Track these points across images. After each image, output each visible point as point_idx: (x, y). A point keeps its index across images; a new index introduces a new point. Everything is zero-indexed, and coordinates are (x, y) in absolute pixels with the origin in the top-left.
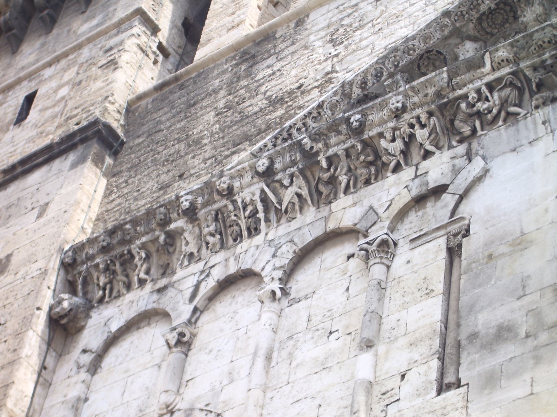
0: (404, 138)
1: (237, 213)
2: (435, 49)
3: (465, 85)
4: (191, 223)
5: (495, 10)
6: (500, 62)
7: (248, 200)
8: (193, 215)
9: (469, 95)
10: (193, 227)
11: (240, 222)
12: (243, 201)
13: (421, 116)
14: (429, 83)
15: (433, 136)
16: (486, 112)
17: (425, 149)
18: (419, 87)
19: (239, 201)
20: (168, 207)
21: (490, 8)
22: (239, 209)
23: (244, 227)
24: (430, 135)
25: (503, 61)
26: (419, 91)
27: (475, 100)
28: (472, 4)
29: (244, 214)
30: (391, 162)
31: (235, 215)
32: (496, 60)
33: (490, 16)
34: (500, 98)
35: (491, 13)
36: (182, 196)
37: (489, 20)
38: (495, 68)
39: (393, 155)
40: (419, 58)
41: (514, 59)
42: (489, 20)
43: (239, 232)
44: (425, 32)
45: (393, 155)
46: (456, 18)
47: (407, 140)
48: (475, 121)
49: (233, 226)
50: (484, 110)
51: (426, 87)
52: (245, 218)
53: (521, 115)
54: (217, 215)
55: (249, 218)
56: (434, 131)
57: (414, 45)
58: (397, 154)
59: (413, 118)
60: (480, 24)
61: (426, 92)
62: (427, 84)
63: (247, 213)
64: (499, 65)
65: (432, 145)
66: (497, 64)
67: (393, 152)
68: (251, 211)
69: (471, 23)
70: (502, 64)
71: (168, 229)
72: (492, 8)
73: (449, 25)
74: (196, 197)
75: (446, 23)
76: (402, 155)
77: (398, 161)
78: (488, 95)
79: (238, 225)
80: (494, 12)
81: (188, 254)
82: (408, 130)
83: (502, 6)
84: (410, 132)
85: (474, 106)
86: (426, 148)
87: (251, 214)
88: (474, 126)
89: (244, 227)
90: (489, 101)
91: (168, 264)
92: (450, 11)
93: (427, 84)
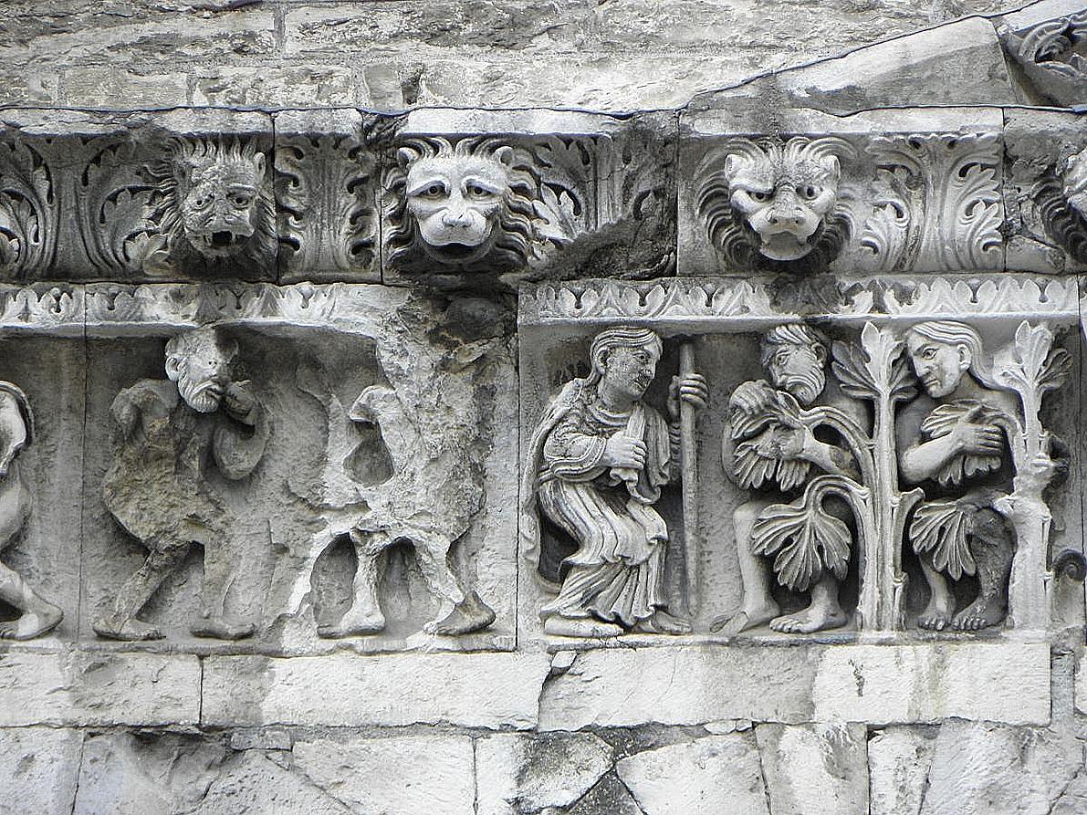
1: (846, 415)
4: (435, 337)
7: (947, 365)
8: (465, 292)
10: (444, 366)
11: (858, 493)
12: (904, 359)
19: (880, 349)
20: (281, 166)
22: (869, 407)
23: (881, 543)
29: (899, 451)
31: (825, 433)
36: (428, 144)
43: (838, 559)
49: (793, 495)
52: (904, 484)
54: (669, 364)
55: (933, 488)
63: (923, 458)
68: (961, 455)
71: (253, 314)
74: (526, 180)
79: (836, 504)
81: (379, 542)
87: (954, 474)
89: (881, 543)
91: (196, 550)
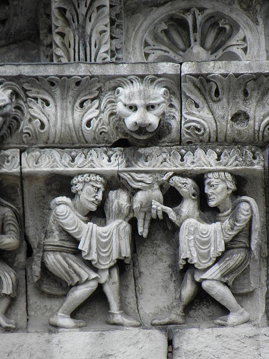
0: (133, 223)
13: (212, 178)
15: (237, 257)
17: (199, 285)
24: (228, 247)
30: (78, 284)
39: (89, 264)
45: (89, 264)
47: (143, 230)
51: (246, 94)
58: (105, 264)
61: (243, 108)
65: (226, 284)
67: (94, 256)
76: (115, 273)
77: (100, 286)
82: (158, 206)
84: (165, 214)
93: (250, 84)
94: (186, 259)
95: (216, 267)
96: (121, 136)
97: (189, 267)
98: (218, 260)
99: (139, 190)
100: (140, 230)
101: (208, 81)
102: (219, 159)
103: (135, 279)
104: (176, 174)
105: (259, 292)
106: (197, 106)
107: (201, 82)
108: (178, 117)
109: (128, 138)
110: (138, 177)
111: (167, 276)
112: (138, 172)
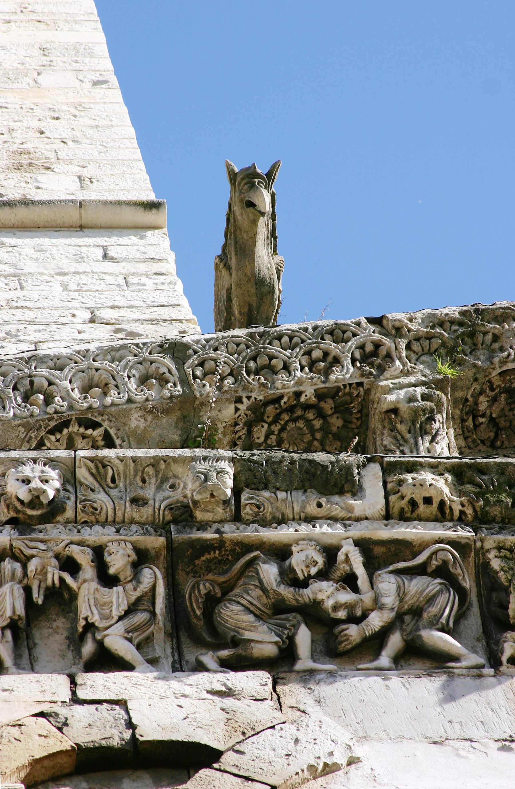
0: (27, 590)
2: (106, 424)
3: (282, 521)
5: (307, 407)
6: (420, 502)
9: (294, 549)
13: (112, 547)
14: (157, 472)
15: (140, 617)
16: (342, 614)
17: (100, 644)
18: (121, 467)
21: (298, 394)
25: (428, 501)
26: (113, 480)
27: (314, 571)
28: (254, 358)
32: (407, 491)
33: (286, 417)
34: (401, 594)
35: (291, 409)
37: (276, 428)
38: (395, 510)
40: (53, 424)
41: (462, 512)
42: (276, 428)
44: (97, 364)
46: (198, 373)
47: (38, 598)
48: (296, 627)
50: (336, 608)
51: (144, 481)
53: (464, 664)
56: (146, 606)
57: (50, 384)
59: (79, 544)
60: (250, 425)
61: (141, 493)
62: (150, 470)
64: (408, 509)
65: (130, 640)
66: (404, 503)
69: (232, 407)
70: (422, 508)
72: (303, 399)
73: (172, 379)
75: (163, 370)
78: (360, 571)
80: (299, 412)
83: (328, 406)
84: (62, 580)
85: (304, 584)
86: (108, 642)
88: (291, 639)
90: (356, 590)
92: (186, 346)
94: (86, 619)
95: (120, 623)
96: (12, 514)
97: (90, 627)
98: (120, 618)
99: (33, 556)
100: (35, 595)
101: (104, 466)
102: (118, 531)
103: (30, 650)
104: (72, 543)
105: (163, 661)
106: (92, 490)
107: (97, 467)
108: (73, 498)
109: (20, 516)
110: (32, 544)
111: (64, 647)
112: (32, 540)
